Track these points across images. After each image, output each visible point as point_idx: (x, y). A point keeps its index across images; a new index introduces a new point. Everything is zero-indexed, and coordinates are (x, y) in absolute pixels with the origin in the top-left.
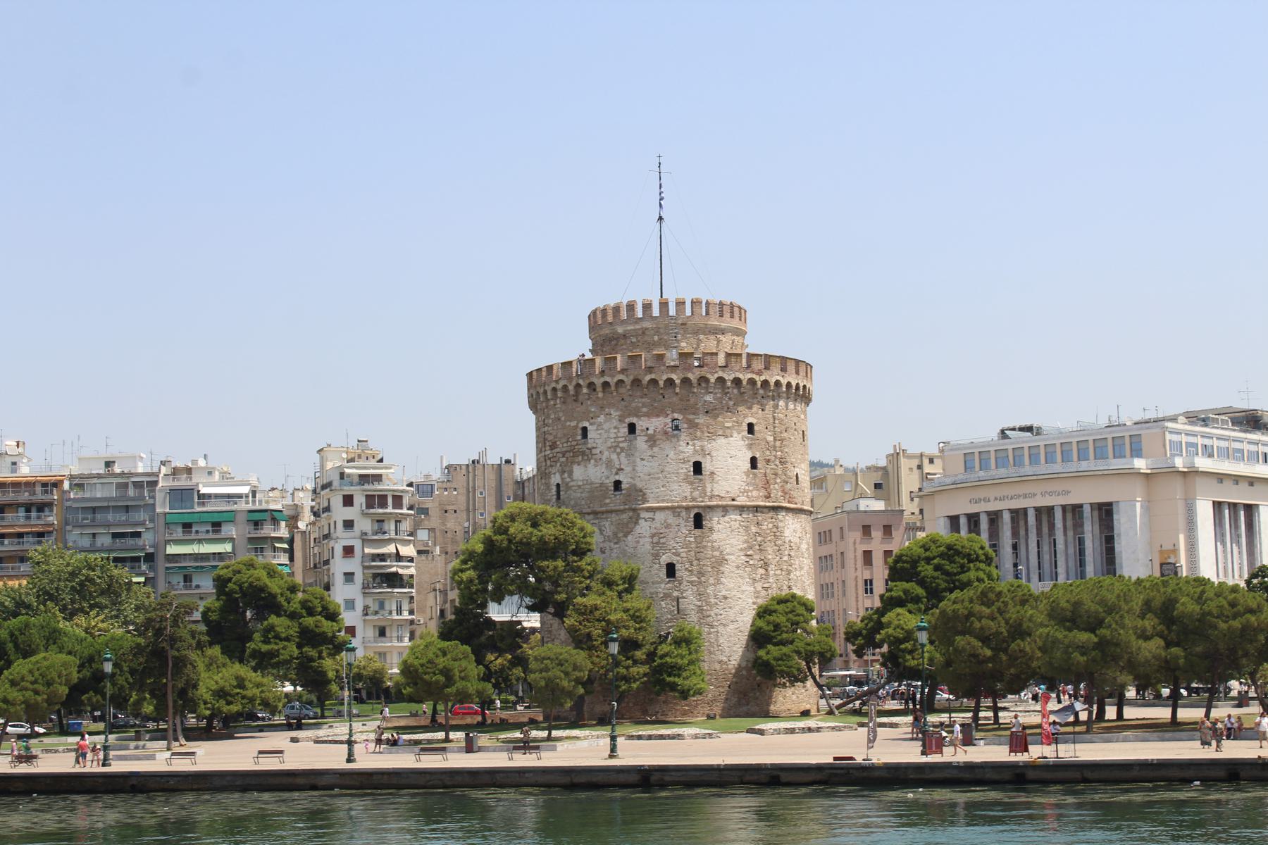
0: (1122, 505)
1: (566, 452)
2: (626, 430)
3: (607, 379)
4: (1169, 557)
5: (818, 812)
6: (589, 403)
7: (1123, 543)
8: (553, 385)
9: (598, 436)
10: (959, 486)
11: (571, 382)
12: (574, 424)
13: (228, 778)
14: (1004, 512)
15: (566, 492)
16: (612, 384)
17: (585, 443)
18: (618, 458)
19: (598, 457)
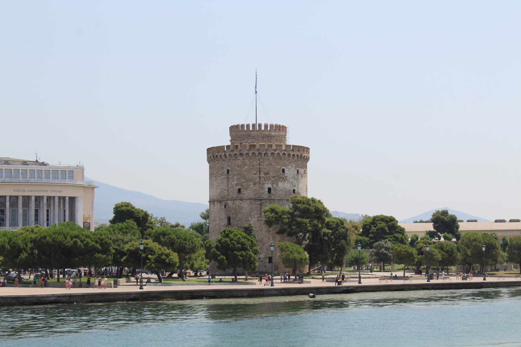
0: (79, 198)
1: (275, 177)
2: (297, 172)
3: (295, 153)
4: (87, 220)
5: (122, 314)
6: (285, 160)
7: (79, 214)
8: (273, 152)
9: (289, 173)
10: (11, 183)
11: (281, 152)
12: (279, 167)
13: (502, 284)
14: (32, 197)
15: (274, 191)
16: (296, 155)
17: (284, 175)
18: (295, 182)
19: (289, 180)
